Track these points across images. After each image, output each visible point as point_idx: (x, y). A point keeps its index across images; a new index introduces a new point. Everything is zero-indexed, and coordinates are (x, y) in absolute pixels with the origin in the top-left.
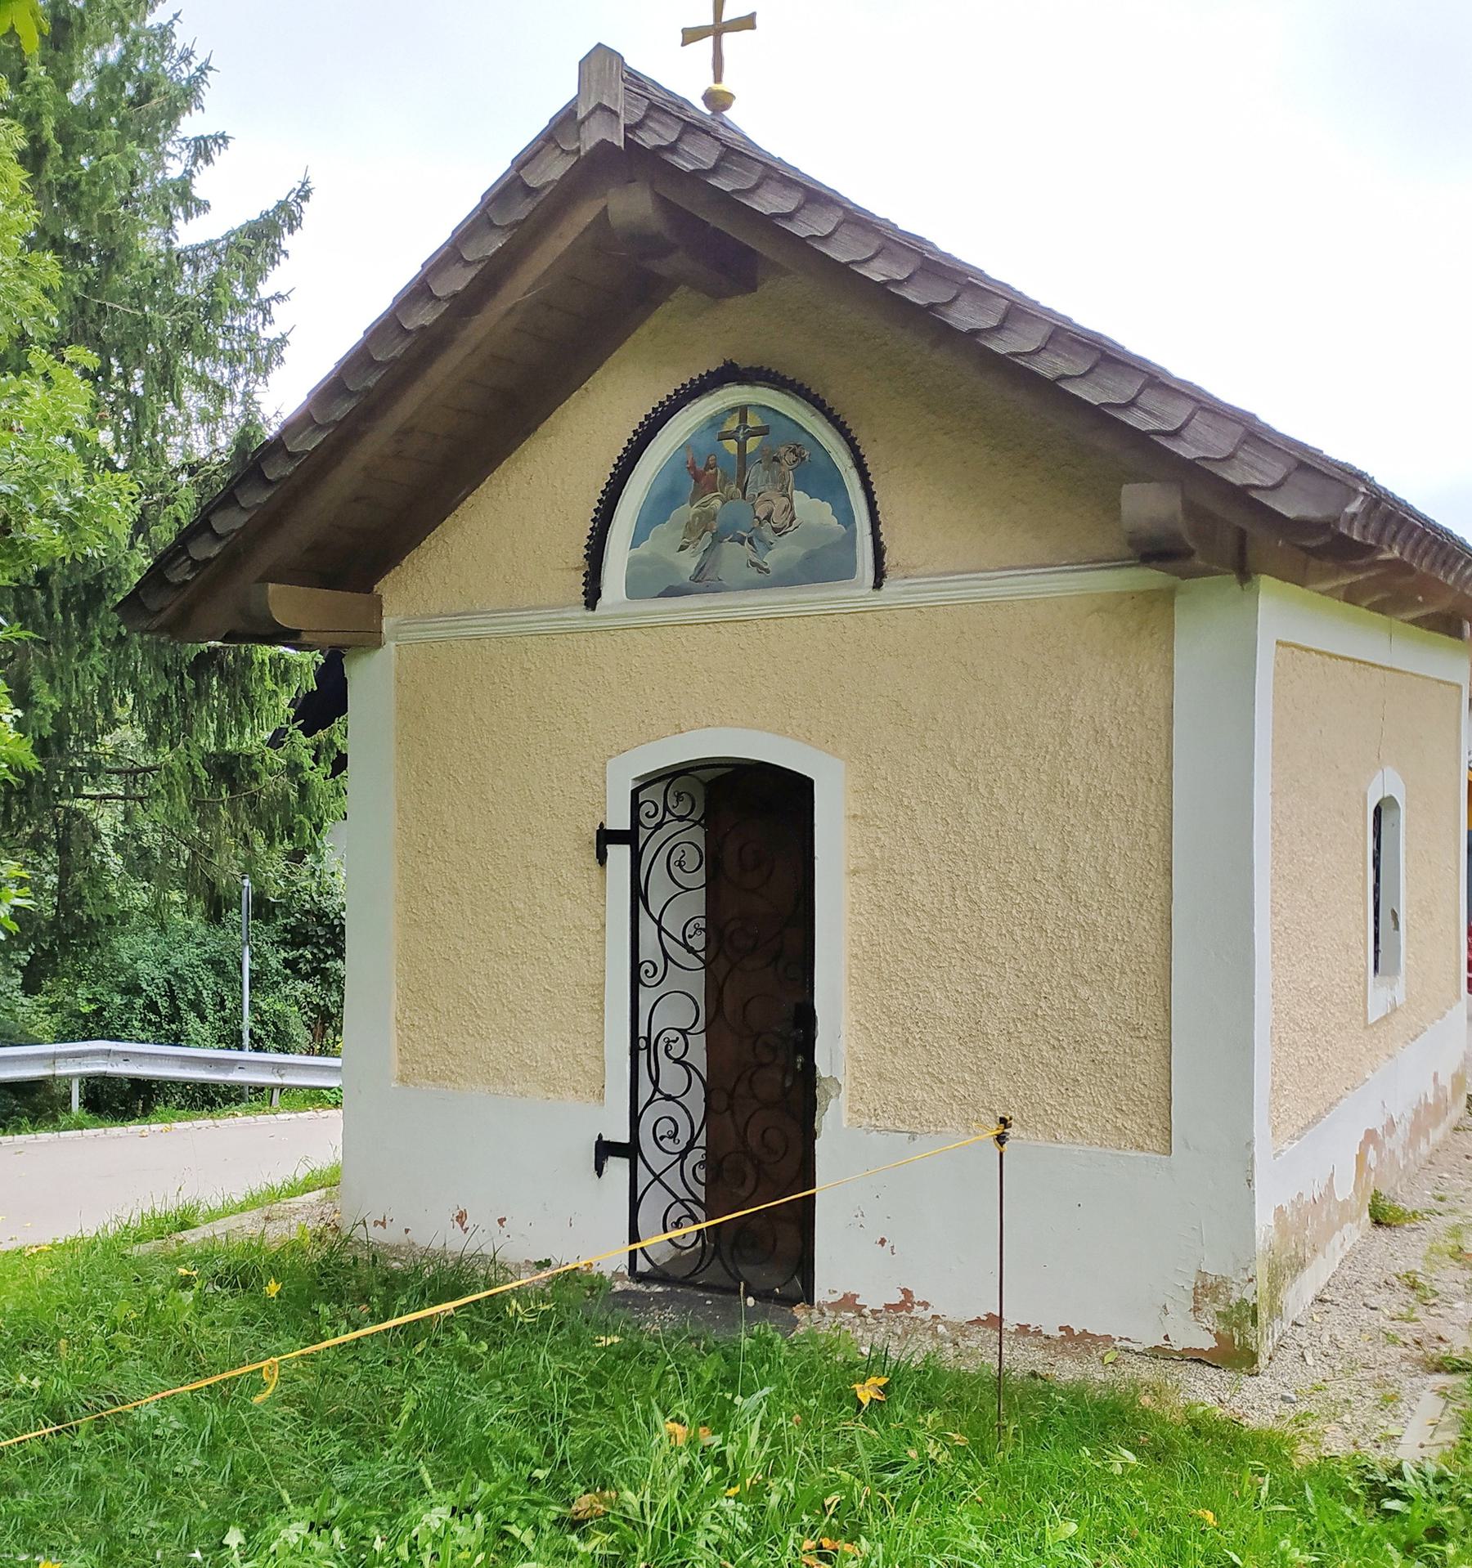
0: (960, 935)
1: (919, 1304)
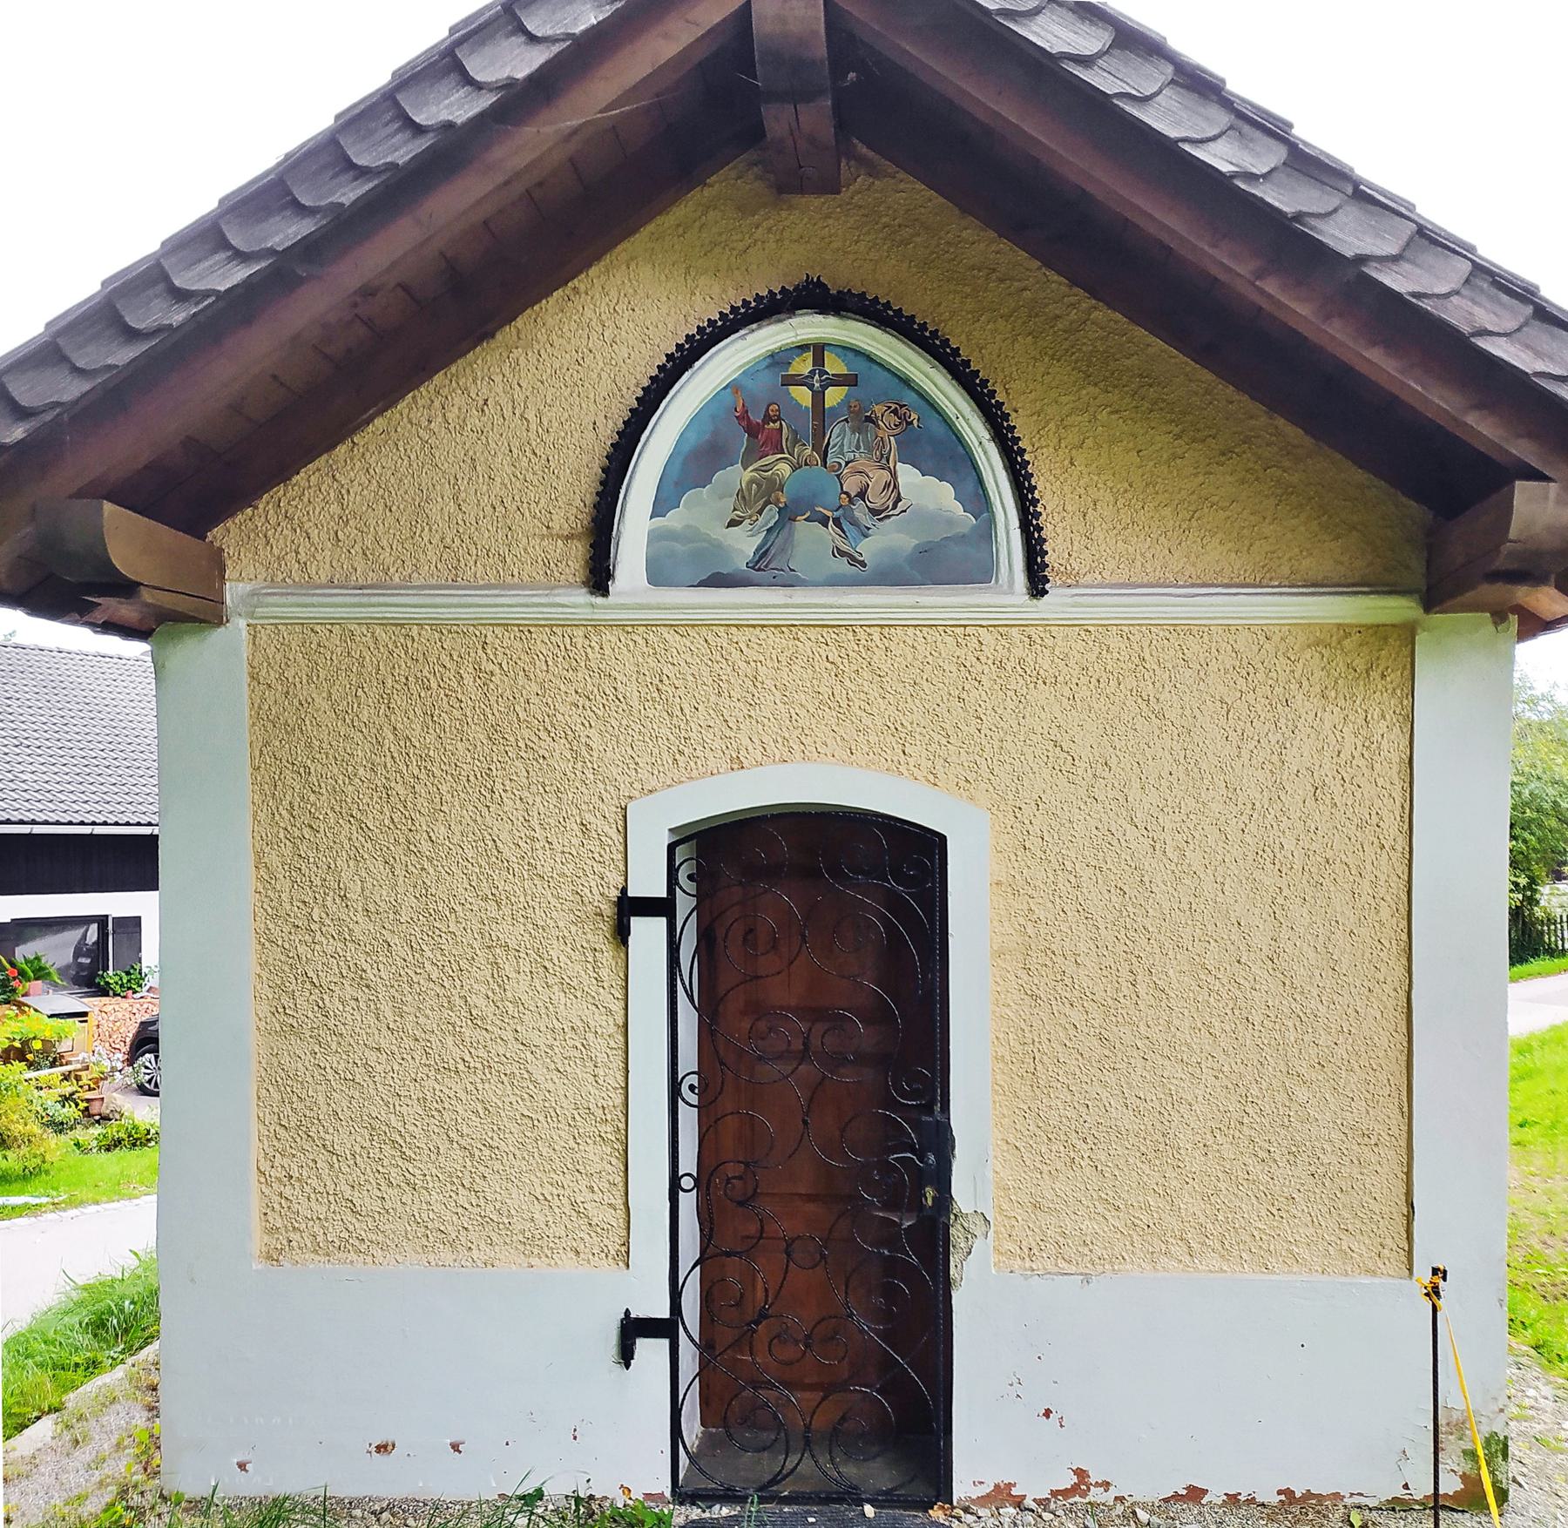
0: (1143, 1028)
1: (1097, 1485)
